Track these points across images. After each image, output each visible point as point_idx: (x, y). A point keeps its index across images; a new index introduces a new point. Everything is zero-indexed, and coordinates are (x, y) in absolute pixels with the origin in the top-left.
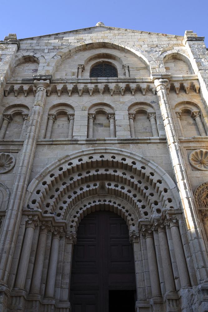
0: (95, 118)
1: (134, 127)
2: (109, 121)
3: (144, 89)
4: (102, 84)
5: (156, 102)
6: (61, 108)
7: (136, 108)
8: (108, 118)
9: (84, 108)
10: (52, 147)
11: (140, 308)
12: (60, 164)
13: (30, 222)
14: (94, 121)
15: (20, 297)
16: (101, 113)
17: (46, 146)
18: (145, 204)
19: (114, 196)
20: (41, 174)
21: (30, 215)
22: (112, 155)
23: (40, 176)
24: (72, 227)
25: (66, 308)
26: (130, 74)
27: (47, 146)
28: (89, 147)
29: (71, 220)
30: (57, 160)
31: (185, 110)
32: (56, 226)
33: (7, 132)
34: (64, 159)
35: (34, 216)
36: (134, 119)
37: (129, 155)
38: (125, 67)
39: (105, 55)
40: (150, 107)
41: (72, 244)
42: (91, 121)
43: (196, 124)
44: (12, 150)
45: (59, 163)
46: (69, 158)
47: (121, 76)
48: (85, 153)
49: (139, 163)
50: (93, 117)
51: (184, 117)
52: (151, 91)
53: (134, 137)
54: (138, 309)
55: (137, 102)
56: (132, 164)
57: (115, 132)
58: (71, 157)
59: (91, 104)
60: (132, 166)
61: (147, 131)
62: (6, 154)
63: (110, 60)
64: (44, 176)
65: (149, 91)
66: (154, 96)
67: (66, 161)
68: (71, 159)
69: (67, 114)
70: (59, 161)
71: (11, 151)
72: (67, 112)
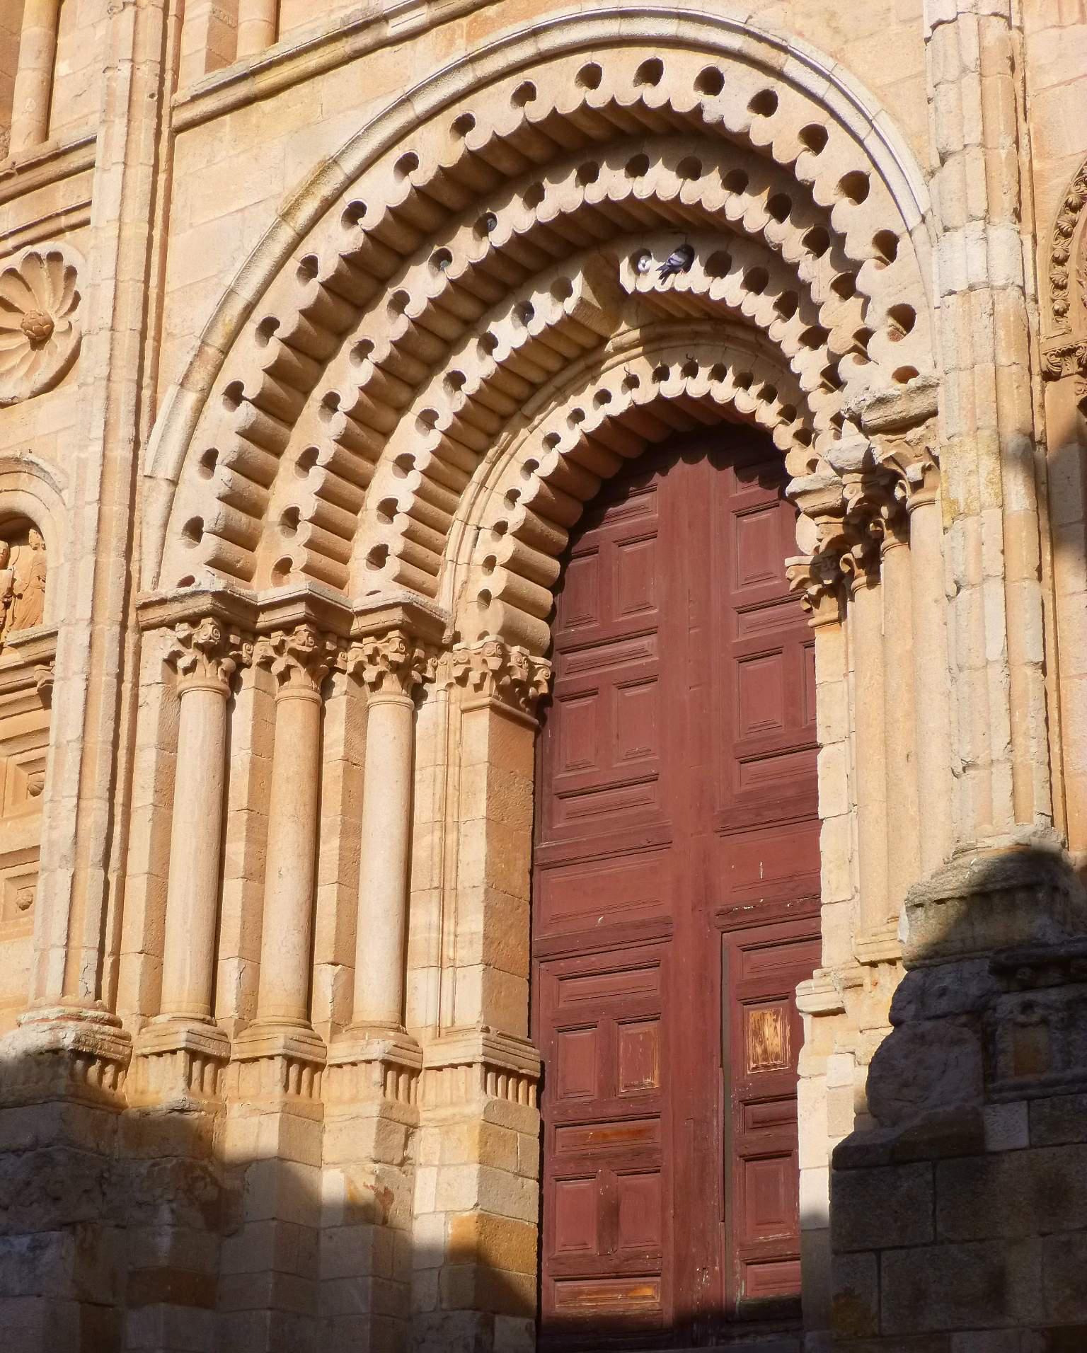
10: (254, 120)
11: (817, 1015)
12: (301, 236)
13: (182, 663)
15: (173, 1052)
17: (223, 125)
19: (706, 328)
20: (204, 343)
21: (182, 620)
22: (582, 60)
23: (199, 353)
24: (485, 596)
25: (469, 1065)
27: (227, 117)
28: (451, 42)
29: (479, 558)
30: (271, 220)
32: (367, 634)
33: (62, 68)
34: (307, 192)
35: (194, 620)
37: (669, 28)
41: (494, 708)
44: (68, 212)
45: (286, 234)
46: (337, 177)
48: (422, 105)
49: (743, 67)
54: (807, 1020)
56: (700, 97)
58: (350, 164)
60: (698, 110)
62: (43, 248)
64: (225, 351)
67: (328, 204)
68: (351, 180)
70: (286, 216)
71: (64, 221)
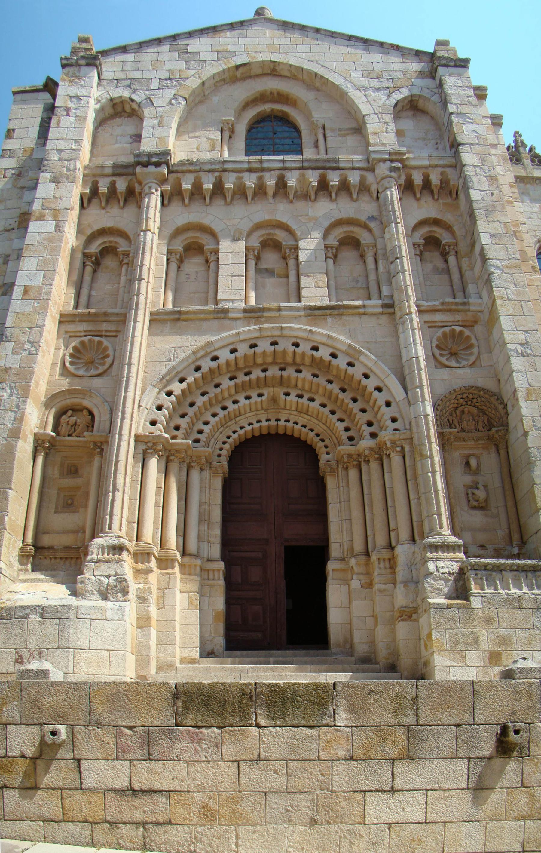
0: (258, 259)
1: (335, 277)
2: (287, 264)
3: (354, 186)
4: (272, 172)
5: (378, 217)
6: (190, 234)
7: (339, 233)
8: (284, 258)
9: (237, 236)
14: (256, 264)
16: (269, 246)
18: (350, 425)
26: (328, 146)
31: (430, 237)
36: (335, 257)
38: (317, 126)
39: (275, 95)
40: (366, 230)
42: (252, 263)
43: (448, 271)
47: (309, 153)
50: (255, 256)
51: (428, 253)
52: (369, 190)
53: (333, 303)
55: (340, 217)
57: (299, 289)
59: (251, 225)
61: (359, 285)
63: (285, 108)
65: (365, 189)
66: (374, 204)
69: (205, 247)
72: (204, 243)
